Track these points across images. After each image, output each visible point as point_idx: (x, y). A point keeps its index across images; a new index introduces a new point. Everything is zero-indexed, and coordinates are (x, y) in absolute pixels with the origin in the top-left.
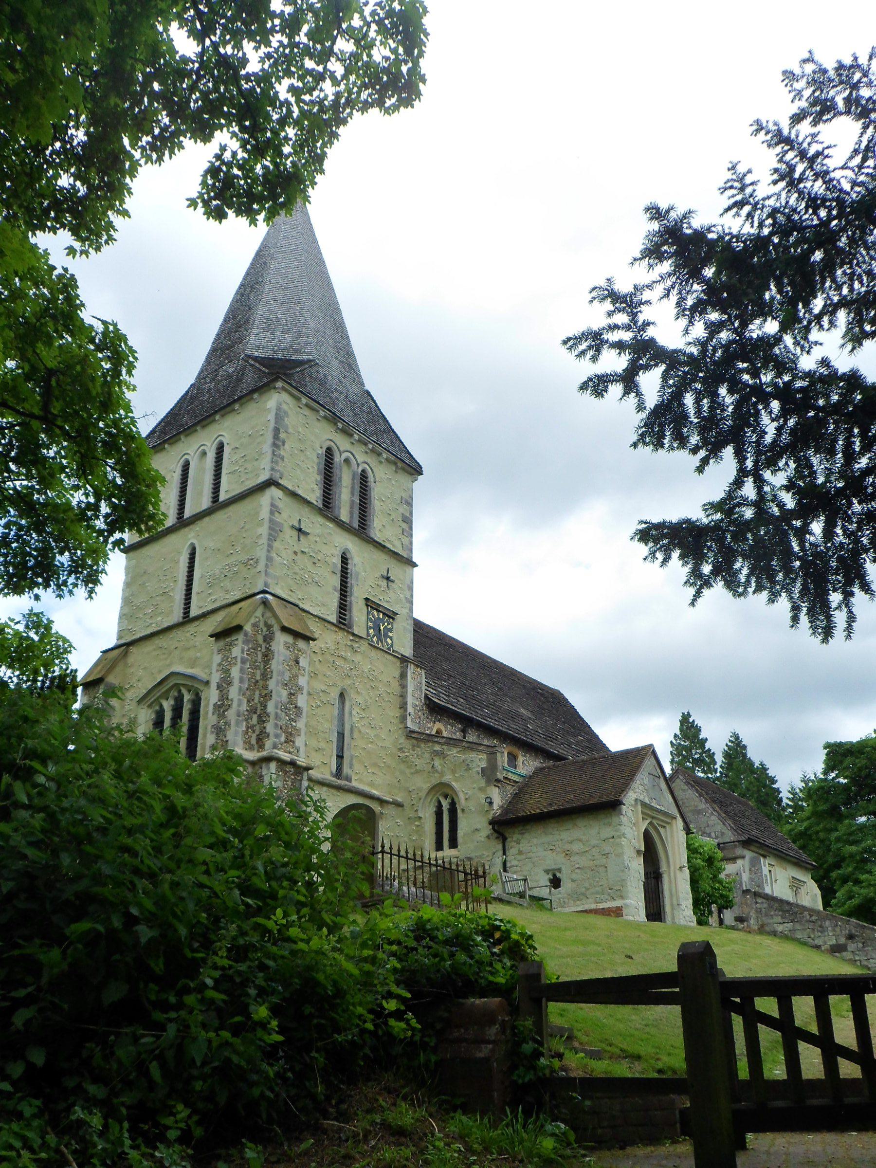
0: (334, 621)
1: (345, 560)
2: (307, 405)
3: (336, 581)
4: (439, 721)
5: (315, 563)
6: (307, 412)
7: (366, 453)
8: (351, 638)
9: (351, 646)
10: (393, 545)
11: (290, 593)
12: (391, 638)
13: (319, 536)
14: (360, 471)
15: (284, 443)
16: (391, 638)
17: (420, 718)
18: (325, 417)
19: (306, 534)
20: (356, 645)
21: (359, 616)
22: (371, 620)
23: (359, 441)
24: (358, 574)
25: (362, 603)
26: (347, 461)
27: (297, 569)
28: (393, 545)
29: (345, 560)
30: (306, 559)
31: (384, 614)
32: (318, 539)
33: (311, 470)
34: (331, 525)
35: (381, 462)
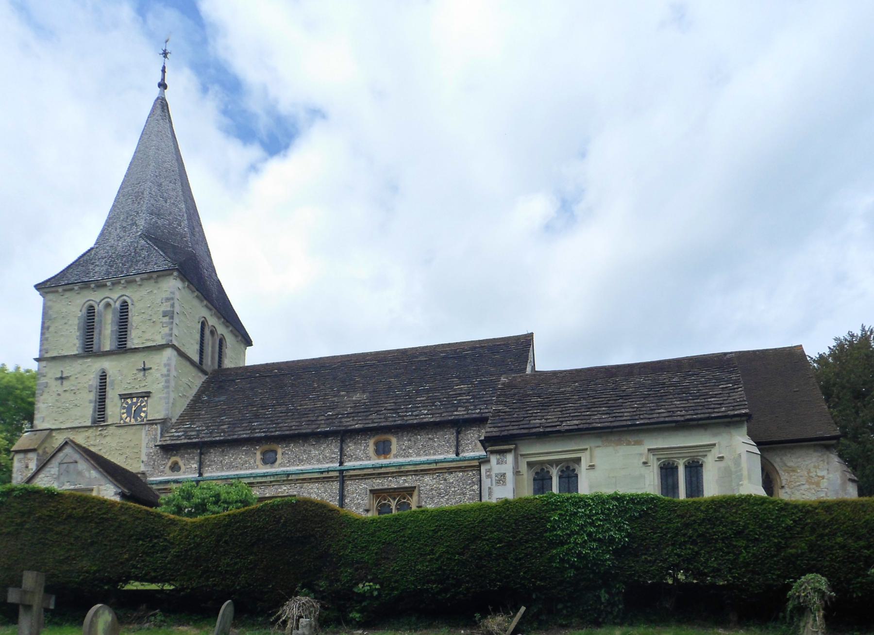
0: (89, 424)
1: (103, 377)
2: (65, 290)
3: (92, 396)
4: (172, 456)
5: (75, 393)
6: (68, 294)
7: (125, 287)
8: (100, 429)
9: (101, 435)
10: (154, 341)
11: (54, 421)
12: (144, 412)
13: (80, 373)
14: (118, 305)
15: (48, 328)
16: (144, 412)
17: (154, 461)
18: (81, 288)
19: (67, 378)
20: (104, 432)
21: (114, 410)
22: (124, 408)
23: (113, 284)
24: (113, 382)
25: (117, 399)
26: (108, 305)
27: (59, 404)
28: (154, 341)
29: (103, 377)
30: (67, 394)
31: (137, 397)
32: (78, 376)
33: (74, 331)
34: (89, 360)
35: (140, 285)
